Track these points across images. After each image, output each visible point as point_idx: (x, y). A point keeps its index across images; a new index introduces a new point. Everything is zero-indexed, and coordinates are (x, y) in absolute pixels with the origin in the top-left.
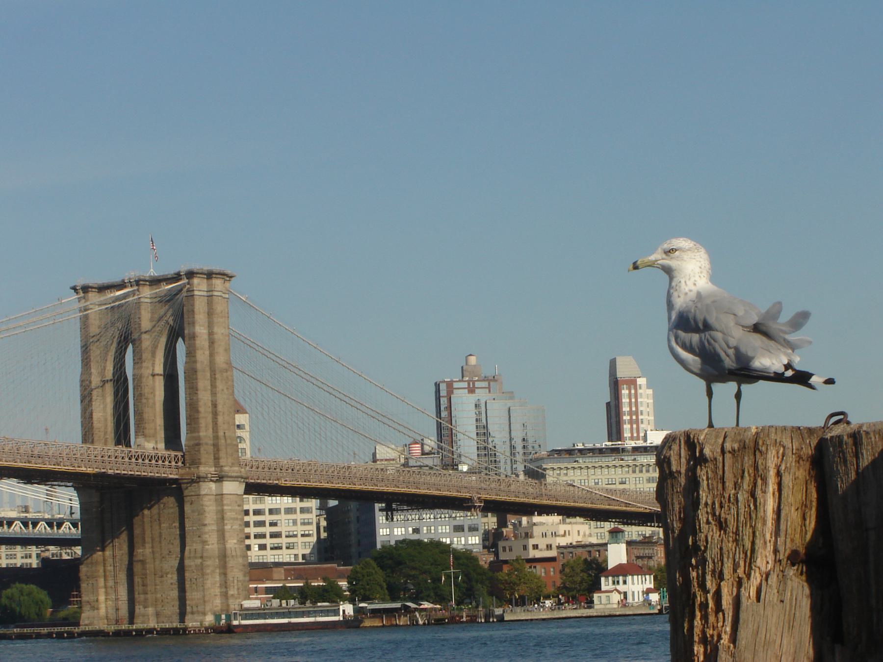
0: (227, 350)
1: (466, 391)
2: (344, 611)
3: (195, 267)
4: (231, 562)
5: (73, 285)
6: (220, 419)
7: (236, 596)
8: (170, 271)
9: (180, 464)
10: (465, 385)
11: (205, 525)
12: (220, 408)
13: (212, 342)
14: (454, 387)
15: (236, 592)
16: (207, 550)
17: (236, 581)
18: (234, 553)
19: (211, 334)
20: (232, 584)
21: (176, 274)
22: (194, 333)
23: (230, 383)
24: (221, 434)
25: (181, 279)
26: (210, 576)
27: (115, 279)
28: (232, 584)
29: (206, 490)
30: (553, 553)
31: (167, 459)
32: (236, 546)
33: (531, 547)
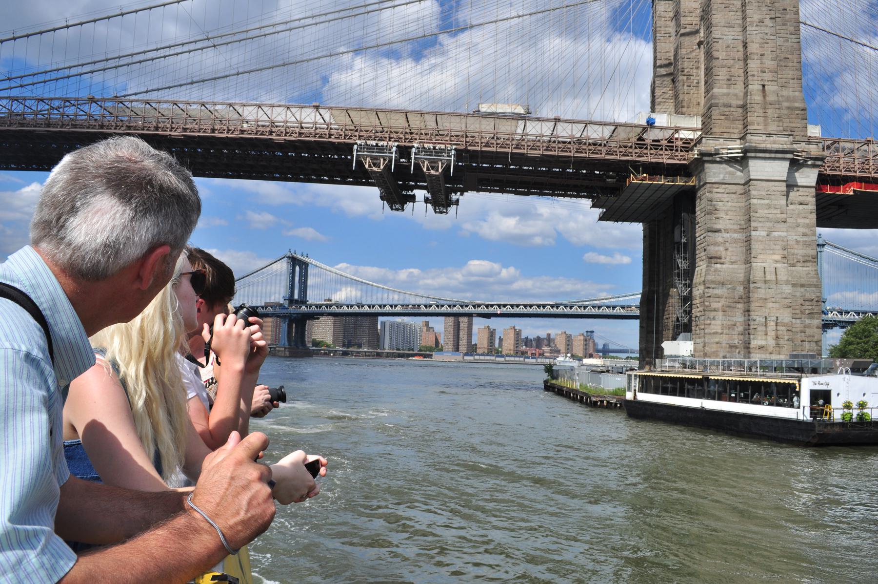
4: (763, 291)
6: (753, 65)
7: (771, 349)
15: (771, 342)
16: (716, 270)
17: (771, 325)
18: (770, 277)
20: (763, 328)
24: (755, 87)
26: (720, 313)
29: (721, 176)
32: (779, 265)
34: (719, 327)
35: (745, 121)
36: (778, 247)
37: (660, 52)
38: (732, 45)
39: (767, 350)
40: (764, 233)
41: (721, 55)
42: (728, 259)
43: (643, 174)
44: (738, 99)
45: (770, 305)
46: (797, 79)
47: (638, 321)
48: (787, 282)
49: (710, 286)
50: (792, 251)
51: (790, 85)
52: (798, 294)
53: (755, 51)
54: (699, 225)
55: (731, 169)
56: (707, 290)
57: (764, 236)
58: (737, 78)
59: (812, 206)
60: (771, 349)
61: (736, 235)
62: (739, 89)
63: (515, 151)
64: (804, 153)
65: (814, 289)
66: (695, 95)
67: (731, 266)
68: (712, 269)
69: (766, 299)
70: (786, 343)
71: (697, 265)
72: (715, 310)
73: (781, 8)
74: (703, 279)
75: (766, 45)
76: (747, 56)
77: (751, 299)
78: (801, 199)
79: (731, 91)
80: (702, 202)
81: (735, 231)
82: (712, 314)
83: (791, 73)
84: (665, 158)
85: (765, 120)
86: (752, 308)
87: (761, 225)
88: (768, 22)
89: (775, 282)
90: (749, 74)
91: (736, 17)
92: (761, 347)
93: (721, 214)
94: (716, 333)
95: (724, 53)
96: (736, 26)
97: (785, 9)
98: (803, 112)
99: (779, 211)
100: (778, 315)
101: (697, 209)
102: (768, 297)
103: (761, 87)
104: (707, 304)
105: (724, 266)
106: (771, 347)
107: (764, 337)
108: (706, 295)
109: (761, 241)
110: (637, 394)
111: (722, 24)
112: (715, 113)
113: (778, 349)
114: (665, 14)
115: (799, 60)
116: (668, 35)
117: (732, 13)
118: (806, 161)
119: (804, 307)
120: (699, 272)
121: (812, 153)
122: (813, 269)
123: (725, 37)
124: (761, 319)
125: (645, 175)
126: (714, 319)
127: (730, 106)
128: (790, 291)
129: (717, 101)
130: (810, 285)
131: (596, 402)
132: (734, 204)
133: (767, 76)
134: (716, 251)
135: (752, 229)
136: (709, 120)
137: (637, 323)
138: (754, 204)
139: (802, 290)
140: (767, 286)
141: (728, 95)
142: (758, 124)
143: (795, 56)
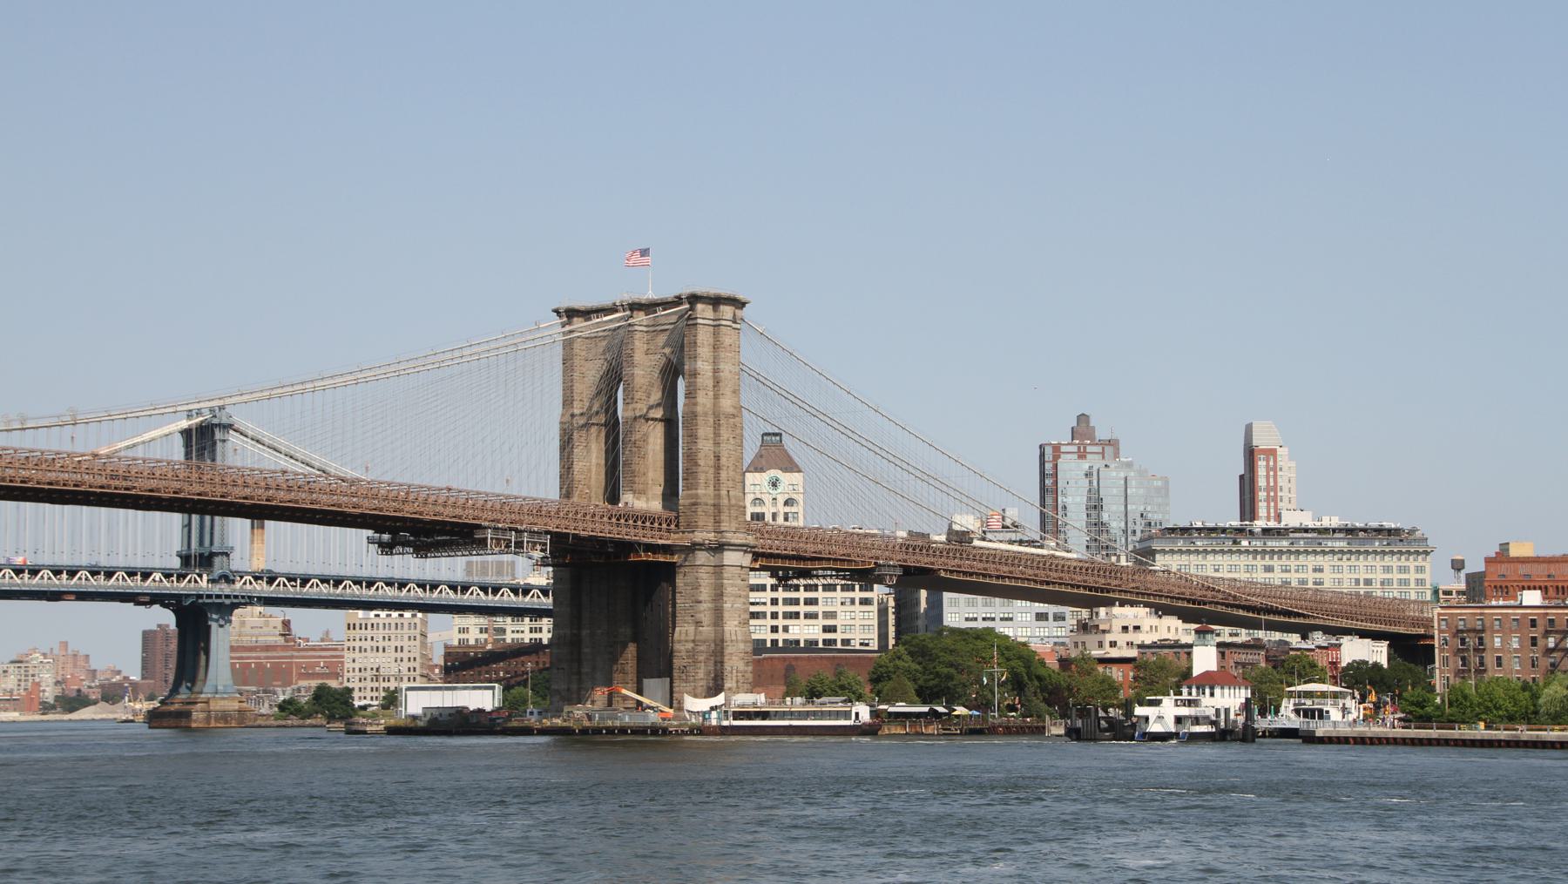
0: (736, 392)
1: (1076, 456)
2: (857, 714)
3: (700, 289)
4: (730, 648)
5: (555, 307)
6: (723, 475)
7: (734, 690)
8: (669, 294)
9: (673, 526)
10: (1074, 449)
11: (700, 602)
12: (723, 461)
13: (717, 383)
14: (1062, 450)
15: (735, 685)
17: (734, 671)
18: (734, 638)
19: (716, 371)
20: (729, 675)
21: (676, 297)
22: (695, 370)
23: (738, 431)
24: (724, 492)
25: (681, 304)
26: (703, 664)
27: (606, 301)
28: (729, 675)
29: (703, 560)
30: (1133, 653)
31: (656, 520)
32: (737, 629)
33: (1108, 645)
40: (730, 605)
61: (710, 605)
79: (707, 492)
86: (725, 661)
111: (703, 437)
141: (705, 495)
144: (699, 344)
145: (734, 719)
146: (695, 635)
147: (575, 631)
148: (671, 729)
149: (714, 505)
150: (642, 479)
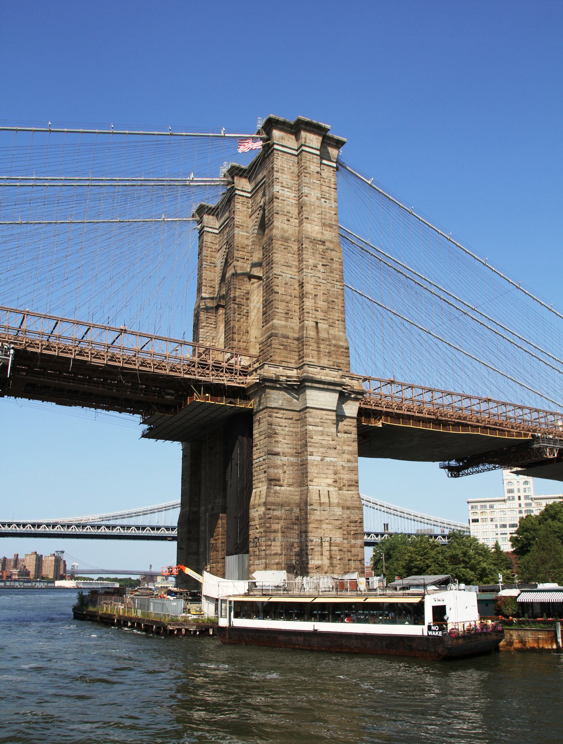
4: (318, 513)
6: (309, 303)
7: (326, 569)
11: (277, 454)
15: (326, 562)
16: (276, 492)
17: (326, 544)
18: (324, 499)
20: (318, 549)
24: (310, 323)
26: (280, 535)
29: (280, 402)
32: (331, 489)
34: (279, 548)
35: (301, 353)
36: (330, 472)
37: (206, 279)
38: (289, 283)
39: (322, 569)
40: (319, 458)
41: (281, 290)
42: (286, 481)
43: (205, 394)
44: (294, 332)
45: (325, 526)
46: (342, 321)
47: (175, 543)
48: (338, 505)
49: (270, 507)
50: (339, 475)
51: (336, 325)
52: (345, 516)
53: (310, 291)
54: (258, 447)
55: (288, 396)
56: (268, 511)
57: (318, 461)
58: (294, 313)
59: (354, 436)
60: (326, 569)
61: (292, 459)
62: (295, 323)
63: (78, 357)
64: (348, 387)
65: (357, 511)
66: (245, 324)
67: (288, 489)
68: (272, 491)
69: (321, 521)
70: (338, 562)
71: (254, 486)
72: (275, 531)
73: (329, 258)
74: (263, 500)
75: (319, 287)
76: (303, 294)
77: (309, 521)
78: (346, 428)
79: (289, 324)
80: (261, 425)
81: (292, 456)
82: (272, 535)
83: (336, 314)
84: (225, 380)
85: (318, 354)
86: (310, 529)
87: (316, 450)
88: (320, 267)
89: (328, 505)
90: (305, 311)
91: (293, 258)
92: (318, 567)
93: (280, 438)
94: (276, 554)
95: (283, 289)
96: (293, 266)
97: (332, 259)
98: (346, 351)
99: (330, 438)
100: (331, 536)
101: (254, 432)
102: (323, 518)
103: (314, 324)
104: (268, 525)
105: (282, 488)
106: (326, 567)
107: (320, 557)
108: (267, 516)
109: (316, 465)
110: (233, 619)
111: (282, 263)
112: (275, 342)
113: (331, 568)
114: (212, 245)
115: (343, 305)
116: (213, 265)
117: (289, 255)
118: (350, 394)
119: (349, 528)
120: (258, 493)
121: (355, 387)
122: (356, 492)
123: (284, 275)
124: (317, 540)
125: (207, 395)
126: (274, 540)
127: (288, 338)
128: (341, 513)
129: (276, 332)
130: (354, 508)
131: (173, 631)
132: (291, 429)
133: (320, 315)
134: (276, 474)
135: (309, 453)
136: (269, 348)
137: (175, 544)
138: (310, 431)
139: (348, 512)
140: (322, 508)
141: (286, 327)
142: (313, 357)
143: (340, 301)
144: (276, 169)
145: (236, 616)
146: (267, 496)
147: (195, 509)
148: (171, 628)
149: (298, 339)
150: (244, 337)
